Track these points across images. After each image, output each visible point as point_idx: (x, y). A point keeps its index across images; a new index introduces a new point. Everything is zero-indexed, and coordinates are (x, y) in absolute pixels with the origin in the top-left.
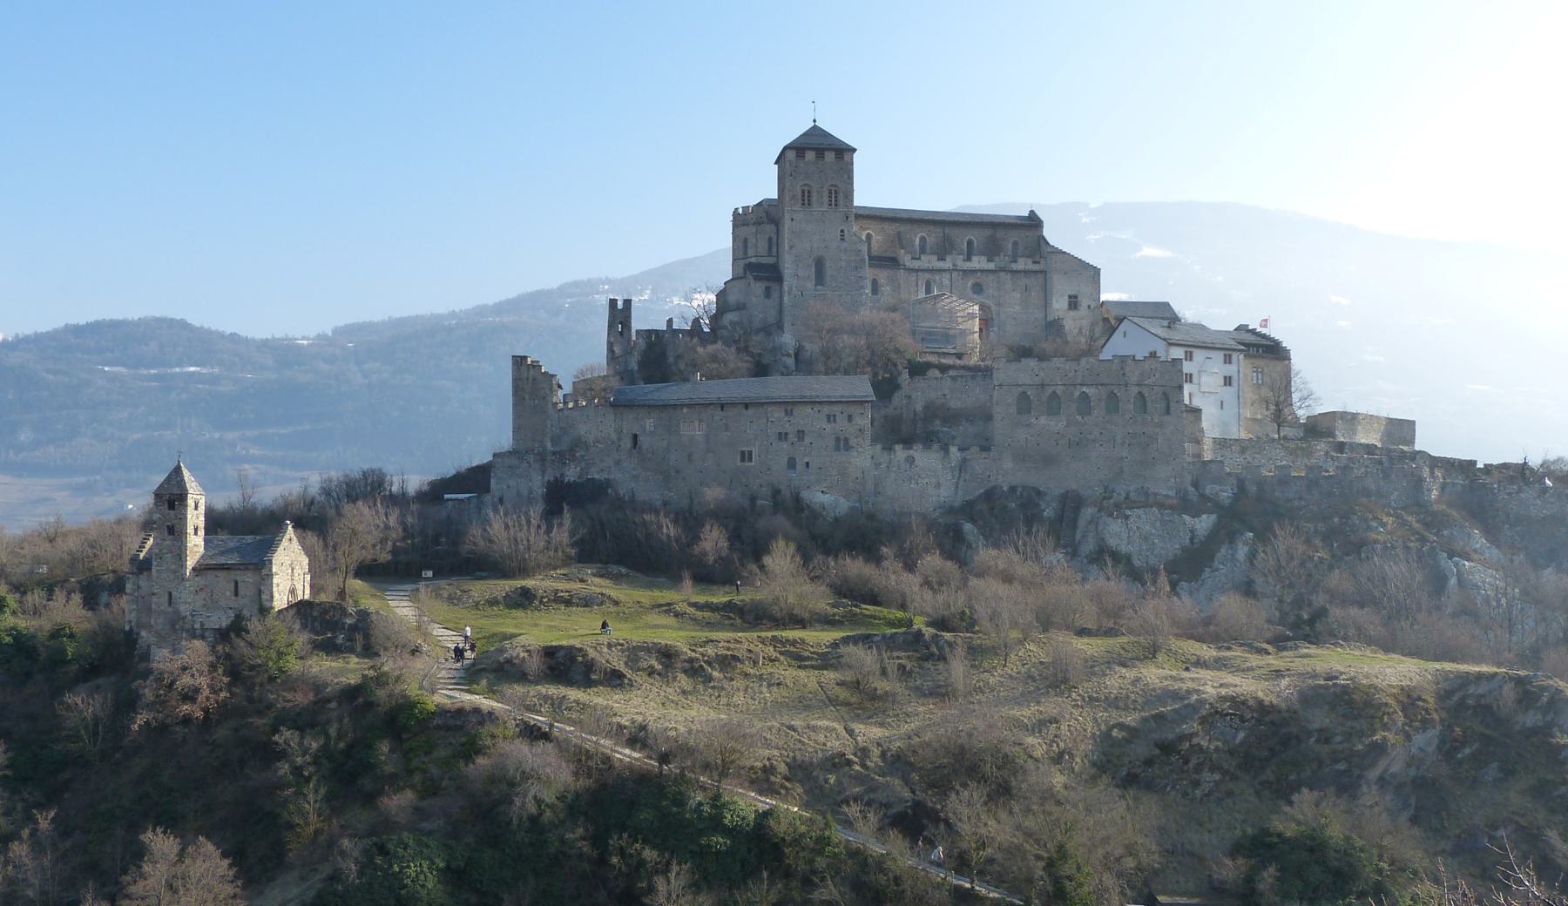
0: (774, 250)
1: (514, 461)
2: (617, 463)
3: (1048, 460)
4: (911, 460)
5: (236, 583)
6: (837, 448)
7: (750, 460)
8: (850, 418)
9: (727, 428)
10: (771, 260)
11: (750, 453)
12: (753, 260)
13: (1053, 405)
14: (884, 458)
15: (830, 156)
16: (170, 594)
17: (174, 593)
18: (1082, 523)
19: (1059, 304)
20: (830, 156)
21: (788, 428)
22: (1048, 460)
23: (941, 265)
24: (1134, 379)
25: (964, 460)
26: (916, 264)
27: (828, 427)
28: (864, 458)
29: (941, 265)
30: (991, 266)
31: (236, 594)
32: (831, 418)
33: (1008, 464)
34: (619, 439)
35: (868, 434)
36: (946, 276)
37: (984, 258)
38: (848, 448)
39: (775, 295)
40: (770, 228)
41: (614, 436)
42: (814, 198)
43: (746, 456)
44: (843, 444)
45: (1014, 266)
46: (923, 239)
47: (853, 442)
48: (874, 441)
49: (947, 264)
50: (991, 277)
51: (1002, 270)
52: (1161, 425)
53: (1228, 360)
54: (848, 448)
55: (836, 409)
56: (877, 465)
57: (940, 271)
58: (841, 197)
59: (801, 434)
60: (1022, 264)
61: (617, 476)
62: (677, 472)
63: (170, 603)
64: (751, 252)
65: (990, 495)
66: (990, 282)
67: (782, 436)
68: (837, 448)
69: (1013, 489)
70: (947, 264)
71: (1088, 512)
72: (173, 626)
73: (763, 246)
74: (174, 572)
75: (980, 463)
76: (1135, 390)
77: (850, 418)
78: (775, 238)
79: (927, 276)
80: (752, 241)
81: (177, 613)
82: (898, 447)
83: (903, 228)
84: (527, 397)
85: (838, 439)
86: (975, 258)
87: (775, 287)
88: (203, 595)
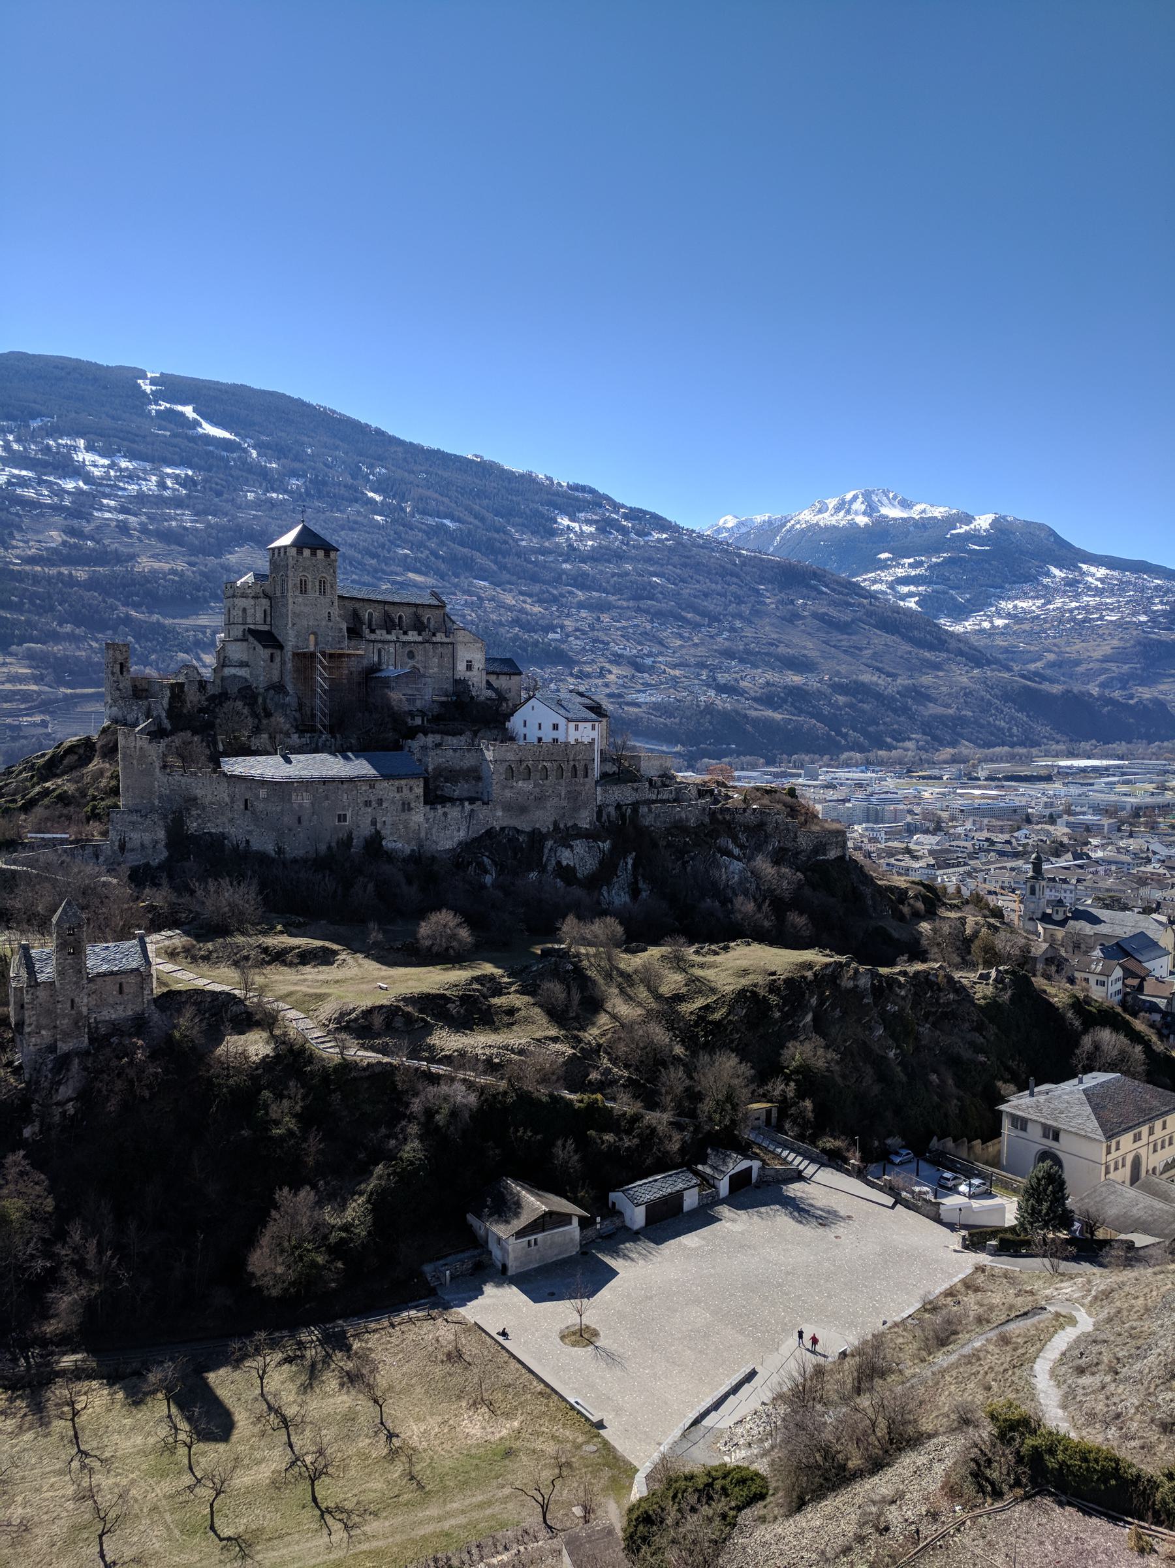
0: (268, 619)
1: (134, 818)
2: (231, 820)
3: (523, 810)
4: (445, 814)
5: (121, 985)
6: (403, 810)
7: (345, 820)
8: (411, 789)
9: (327, 798)
10: (266, 628)
11: (345, 815)
12: (252, 627)
13: (528, 774)
14: (431, 815)
15: (320, 554)
16: (73, 1001)
17: (77, 1000)
18: (546, 851)
19: (461, 667)
20: (320, 554)
21: (372, 798)
22: (523, 810)
23: (389, 637)
24: (571, 757)
25: (472, 810)
26: (373, 637)
27: (398, 796)
28: (419, 816)
29: (389, 637)
30: (420, 639)
31: (121, 991)
32: (399, 790)
33: (499, 813)
34: (232, 802)
35: (422, 799)
36: (392, 645)
37: (415, 633)
38: (410, 809)
39: (278, 659)
40: (265, 602)
41: (227, 799)
42: (309, 586)
43: (342, 818)
44: (406, 807)
45: (434, 639)
46: (370, 614)
47: (413, 805)
48: (426, 803)
49: (392, 637)
50: (421, 647)
51: (427, 642)
52: (584, 785)
53: (593, 728)
54: (410, 809)
55: (403, 782)
56: (427, 820)
57: (389, 642)
58: (328, 586)
59: (380, 802)
60: (440, 638)
61: (231, 830)
62: (290, 830)
63: (72, 1007)
64: (249, 620)
65: (490, 833)
66: (419, 651)
67: (368, 803)
68: (403, 810)
69: (503, 829)
70: (392, 637)
71: (550, 843)
72: (76, 1023)
73: (260, 616)
74: (76, 983)
75: (482, 812)
76: (572, 763)
77: (411, 789)
78: (268, 612)
79: (380, 646)
80: (250, 612)
81: (80, 1013)
82: (439, 807)
83: (357, 605)
84: (135, 762)
85: (403, 804)
86: (410, 633)
87: (277, 652)
88: (94, 996)
